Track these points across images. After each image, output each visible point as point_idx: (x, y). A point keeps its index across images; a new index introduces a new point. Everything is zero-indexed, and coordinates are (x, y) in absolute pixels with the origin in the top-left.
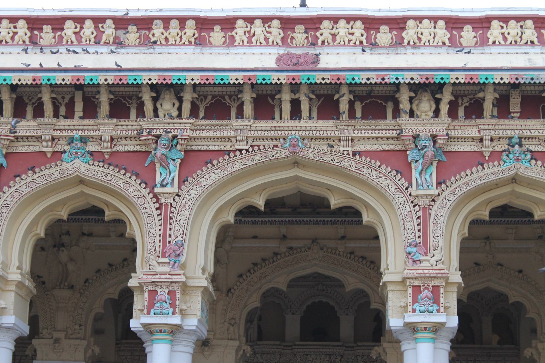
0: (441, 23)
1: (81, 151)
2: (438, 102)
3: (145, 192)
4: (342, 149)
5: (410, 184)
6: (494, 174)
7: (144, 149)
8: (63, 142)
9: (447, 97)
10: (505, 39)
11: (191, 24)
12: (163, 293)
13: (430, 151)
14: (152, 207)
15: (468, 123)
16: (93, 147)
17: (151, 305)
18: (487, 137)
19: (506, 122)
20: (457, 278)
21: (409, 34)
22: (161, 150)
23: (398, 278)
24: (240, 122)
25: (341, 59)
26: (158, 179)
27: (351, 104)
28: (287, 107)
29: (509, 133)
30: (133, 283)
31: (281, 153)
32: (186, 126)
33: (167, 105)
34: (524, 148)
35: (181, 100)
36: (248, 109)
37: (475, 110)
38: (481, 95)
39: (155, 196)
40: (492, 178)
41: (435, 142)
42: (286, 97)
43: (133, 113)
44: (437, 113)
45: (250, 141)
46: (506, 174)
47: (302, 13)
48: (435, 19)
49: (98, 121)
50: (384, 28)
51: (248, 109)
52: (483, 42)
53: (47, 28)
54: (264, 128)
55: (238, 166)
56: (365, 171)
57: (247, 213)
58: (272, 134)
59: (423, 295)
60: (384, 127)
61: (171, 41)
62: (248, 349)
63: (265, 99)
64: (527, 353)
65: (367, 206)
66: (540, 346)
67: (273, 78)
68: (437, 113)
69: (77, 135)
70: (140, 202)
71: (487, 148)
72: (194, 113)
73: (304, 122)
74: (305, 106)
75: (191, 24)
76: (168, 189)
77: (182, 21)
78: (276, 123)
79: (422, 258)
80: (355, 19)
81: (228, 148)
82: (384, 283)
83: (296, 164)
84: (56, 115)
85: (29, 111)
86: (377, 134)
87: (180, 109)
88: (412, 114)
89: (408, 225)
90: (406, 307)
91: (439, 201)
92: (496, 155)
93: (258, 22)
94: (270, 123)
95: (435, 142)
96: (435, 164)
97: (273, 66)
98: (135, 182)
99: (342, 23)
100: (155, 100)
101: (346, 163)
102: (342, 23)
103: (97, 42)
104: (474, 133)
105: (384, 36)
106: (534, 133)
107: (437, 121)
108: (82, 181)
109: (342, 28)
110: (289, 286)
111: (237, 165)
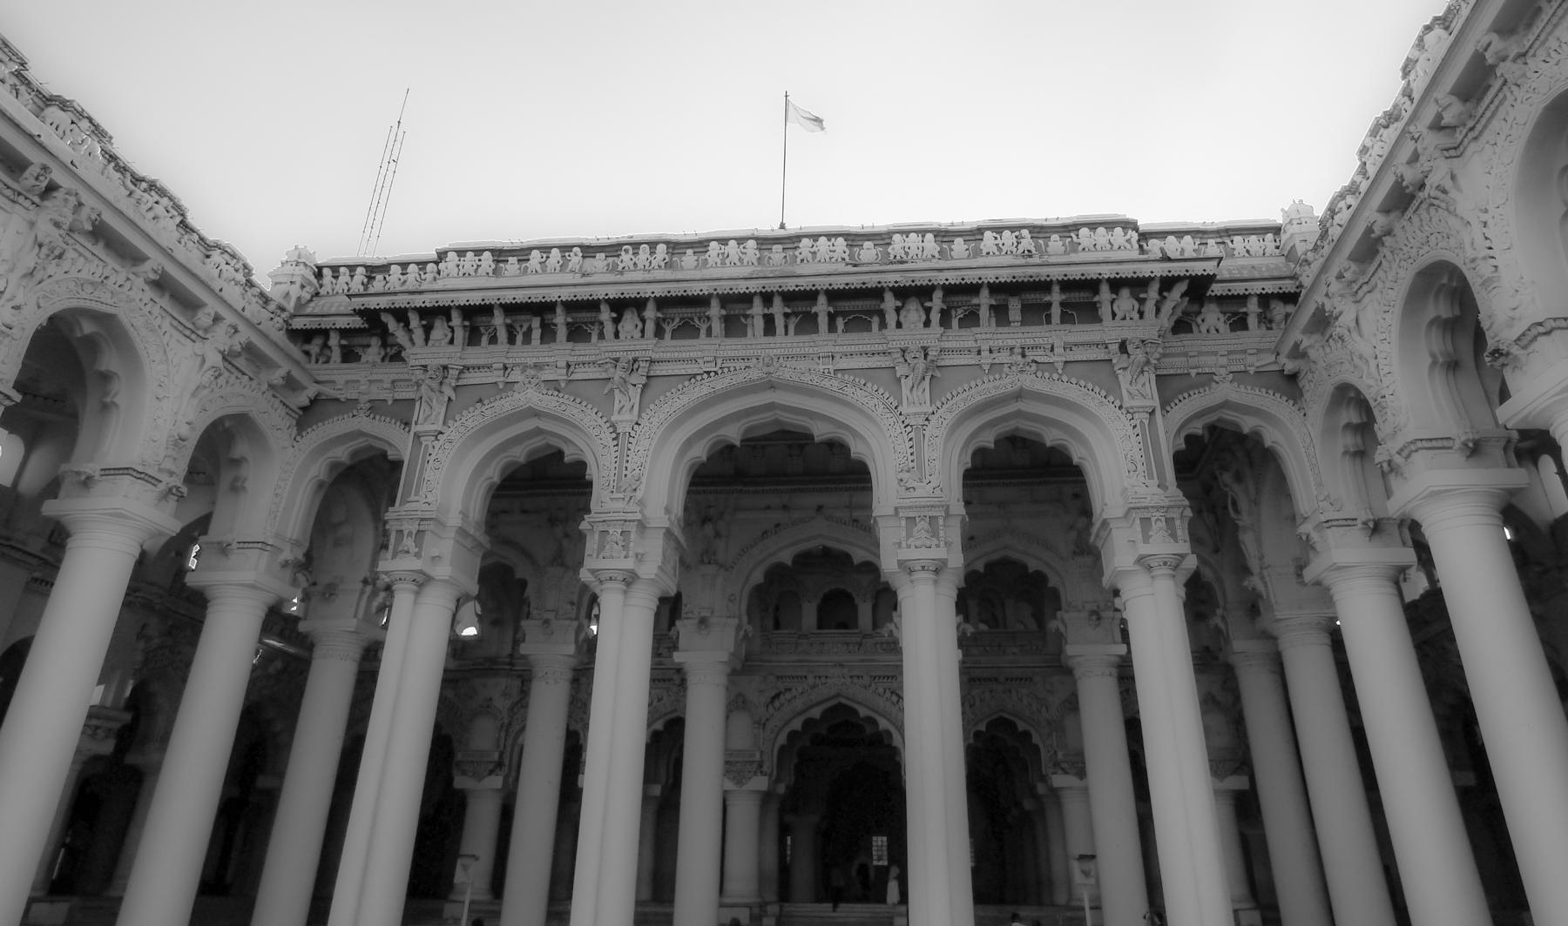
0: (929, 236)
1: (534, 381)
2: (928, 311)
3: (601, 422)
4: (821, 367)
5: (900, 403)
6: (996, 388)
7: (604, 376)
8: (517, 371)
9: (937, 301)
10: (1000, 249)
11: (661, 248)
13: (921, 364)
14: (608, 438)
15: (963, 332)
16: (548, 375)
18: (985, 347)
19: (1006, 329)
24: (708, 340)
26: (617, 406)
27: (832, 318)
28: (759, 323)
29: (1010, 343)
31: (755, 374)
32: (648, 347)
34: (1029, 359)
35: (643, 321)
37: (971, 319)
38: (975, 301)
39: (613, 426)
40: (993, 393)
41: (926, 356)
42: (757, 308)
43: (594, 338)
44: (927, 323)
45: (719, 362)
46: (1010, 389)
47: (782, 233)
48: (922, 232)
49: (553, 345)
50: (868, 244)
51: (717, 327)
56: (849, 390)
57: (725, 451)
58: (742, 353)
59: (919, 526)
60: (870, 340)
61: (640, 266)
62: (749, 628)
64: (1053, 625)
66: (1066, 616)
67: (741, 287)
68: (927, 323)
69: (530, 361)
70: (596, 432)
71: (986, 359)
72: (659, 333)
73: (780, 337)
74: (779, 322)
75: (661, 248)
76: (626, 416)
77: (653, 245)
78: (749, 340)
79: (915, 484)
80: (837, 235)
81: (695, 371)
83: (772, 386)
84: (511, 340)
86: (861, 348)
87: (643, 331)
88: (899, 325)
89: (898, 449)
90: (899, 544)
91: (933, 419)
93: (732, 243)
94: (743, 341)
95: (926, 356)
96: (928, 379)
99: (823, 240)
100: (617, 321)
101: (826, 383)
102: (823, 240)
104: (971, 344)
106: (1039, 341)
107: (927, 331)
108: (534, 413)
110: (794, 562)
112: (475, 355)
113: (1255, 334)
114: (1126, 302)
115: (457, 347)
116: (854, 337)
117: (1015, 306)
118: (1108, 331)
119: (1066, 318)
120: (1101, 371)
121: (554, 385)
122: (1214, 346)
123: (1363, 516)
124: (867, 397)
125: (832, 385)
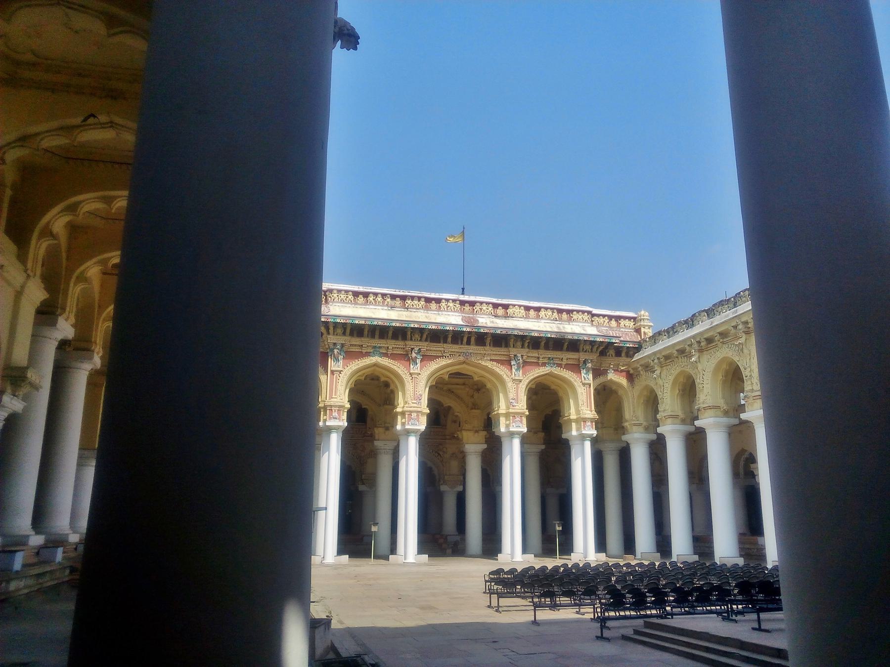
12: (414, 415)
17: (409, 420)
20: (527, 413)
21: (510, 311)
22: (414, 355)
23: (504, 412)
25: (487, 321)
28: (465, 340)
30: (399, 410)
31: (462, 358)
32: (425, 346)
33: (417, 336)
36: (449, 339)
43: (400, 338)
51: (449, 339)
52: (538, 317)
53: (361, 296)
54: (455, 348)
55: (444, 363)
60: (502, 351)
63: (456, 337)
65: (489, 380)
74: (473, 339)
82: (498, 414)
83: (464, 362)
85: (355, 333)
87: (421, 337)
92: (544, 364)
97: (462, 323)
98: (402, 367)
103: (383, 305)
104: (536, 355)
105: (500, 311)
108: (376, 365)
109: (484, 307)
111: (443, 362)
112: (356, 341)
113: (623, 359)
114: (588, 347)
115: (347, 338)
116: (498, 349)
117: (551, 343)
118: (582, 356)
119: (568, 350)
120: (576, 368)
121: (385, 355)
122: (611, 360)
123: (645, 424)
124: (501, 370)
125: (489, 364)
